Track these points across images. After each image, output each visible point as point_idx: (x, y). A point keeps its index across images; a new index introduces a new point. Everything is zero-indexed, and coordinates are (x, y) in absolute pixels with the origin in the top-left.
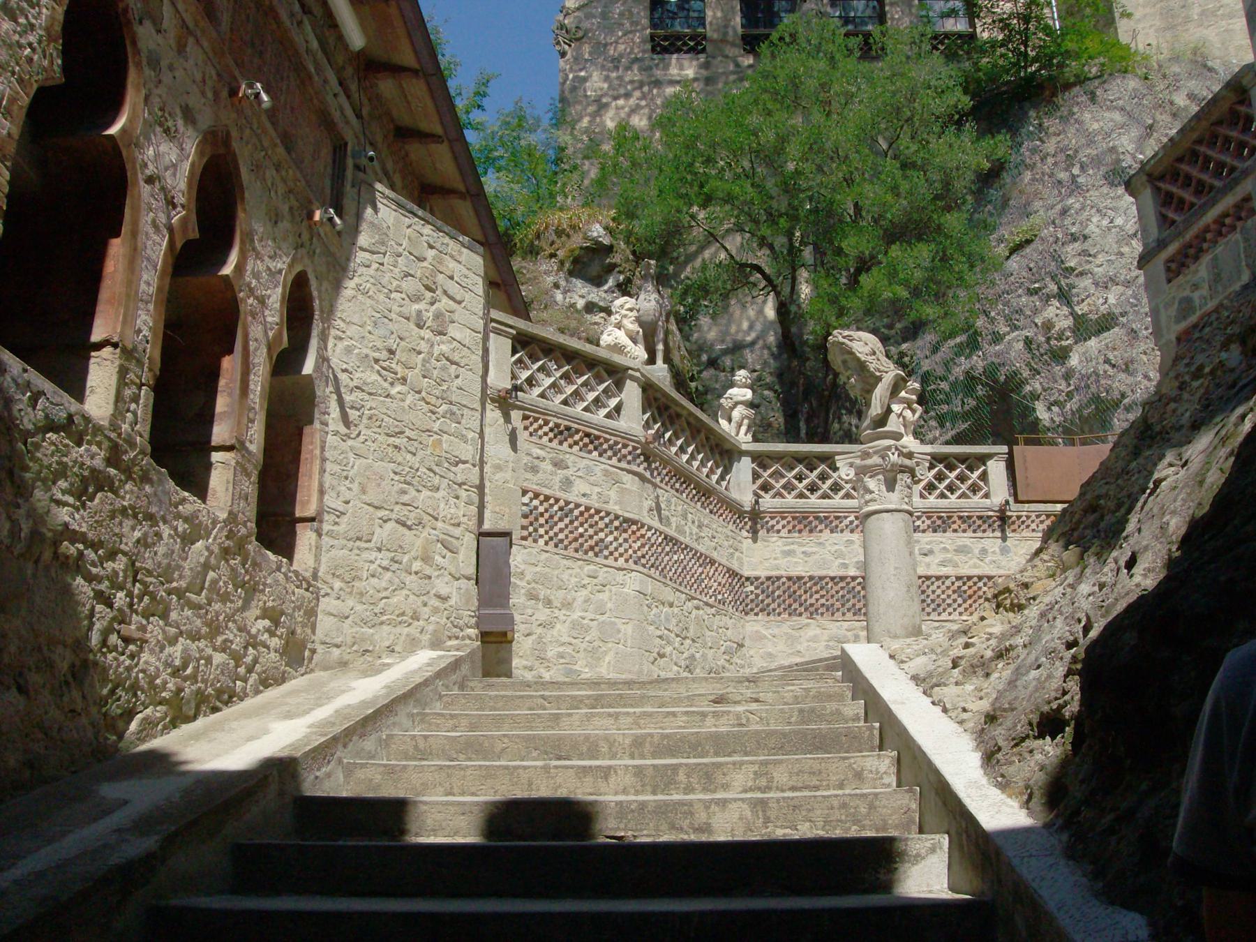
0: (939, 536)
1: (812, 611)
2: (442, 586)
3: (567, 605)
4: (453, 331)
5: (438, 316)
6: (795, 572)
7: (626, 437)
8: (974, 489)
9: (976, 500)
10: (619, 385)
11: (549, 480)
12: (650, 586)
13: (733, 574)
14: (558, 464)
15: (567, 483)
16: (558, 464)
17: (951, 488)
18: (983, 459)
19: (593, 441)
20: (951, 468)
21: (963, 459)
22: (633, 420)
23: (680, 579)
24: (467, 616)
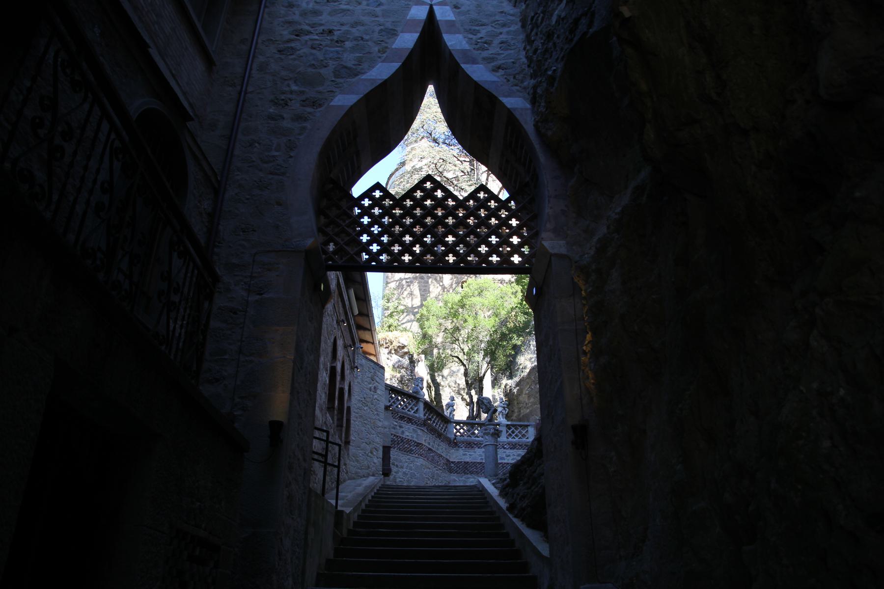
0: (512, 451)
1: (472, 473)
2: (375, 461)
3: (402, 467)
4: (379, 392)
5: (375, 388)
6: (468, 460)
7: (419, 419)
8: (524, 436)
9: (524, 439)
10: (417, 402)
11: (399, 431)
12: (424, 463)
13: (448, 461)
14: (401, 427)
15: (403, 432)
16: (401, 427)
17: (516, 435)
18: (527, 426)
19: (410, 420)
20: (516, 429)
21: (521, 426)
22: (421, 414)
23: (432, 461)
24: (380, 468)
